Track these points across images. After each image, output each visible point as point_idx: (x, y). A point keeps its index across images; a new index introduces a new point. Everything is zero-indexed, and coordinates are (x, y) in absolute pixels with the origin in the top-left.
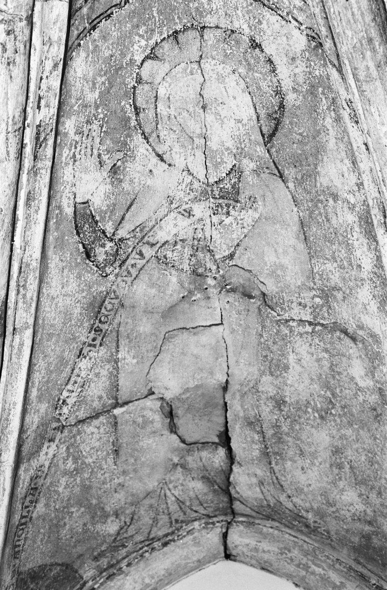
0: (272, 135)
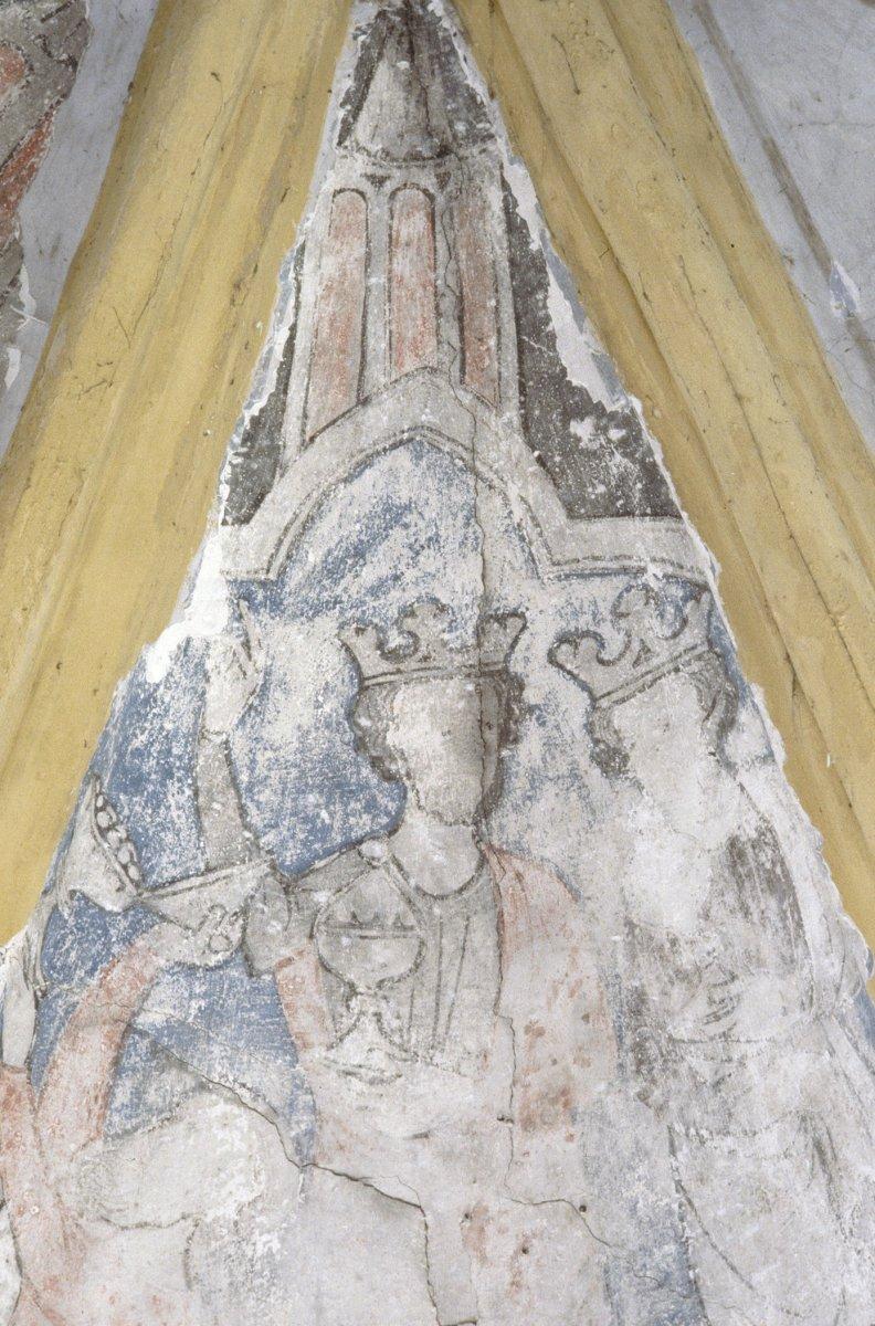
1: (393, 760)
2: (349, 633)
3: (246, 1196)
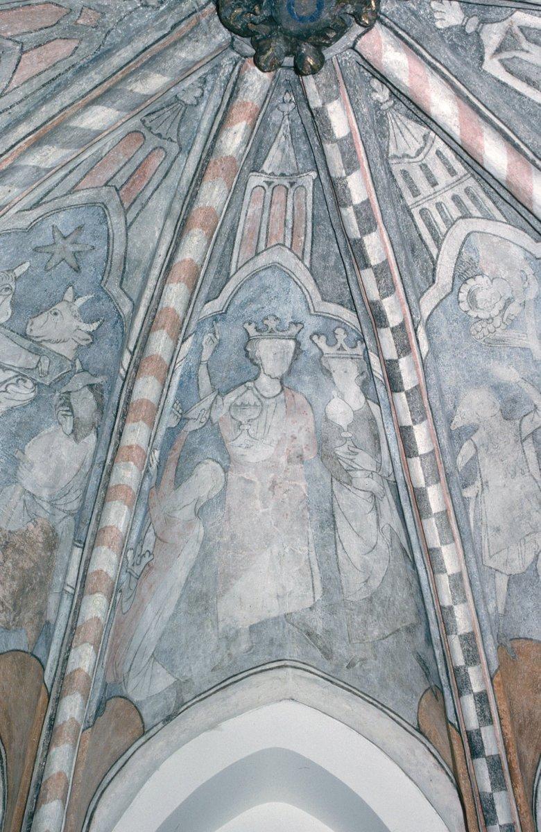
1: (257, 360)
2: (246, 326)
3: (210, 487)
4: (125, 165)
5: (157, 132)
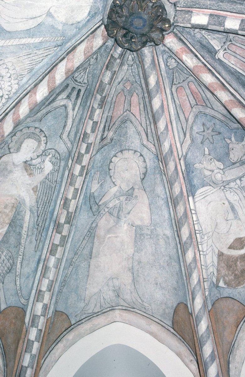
0: (143, 179)
4: (188, 98)
5: (182, 81)
